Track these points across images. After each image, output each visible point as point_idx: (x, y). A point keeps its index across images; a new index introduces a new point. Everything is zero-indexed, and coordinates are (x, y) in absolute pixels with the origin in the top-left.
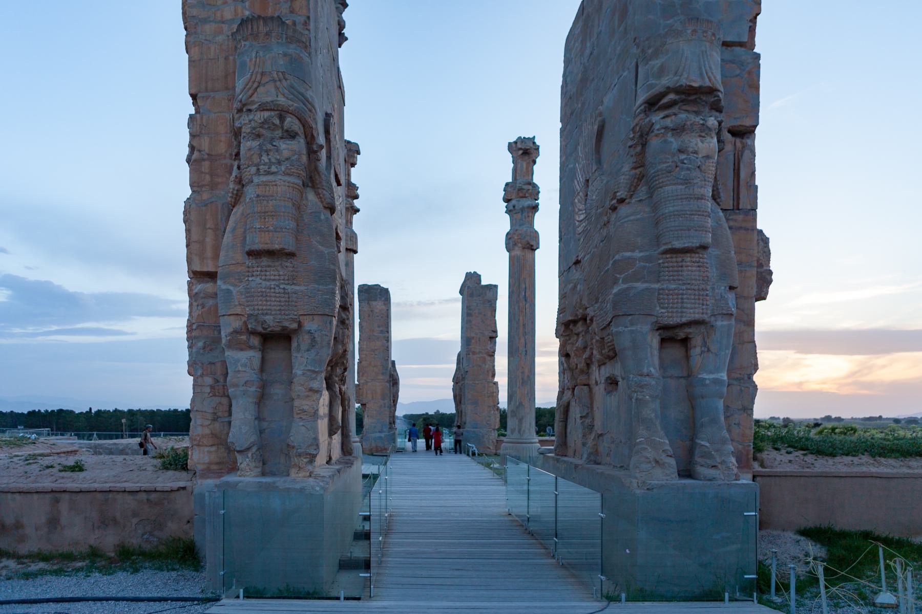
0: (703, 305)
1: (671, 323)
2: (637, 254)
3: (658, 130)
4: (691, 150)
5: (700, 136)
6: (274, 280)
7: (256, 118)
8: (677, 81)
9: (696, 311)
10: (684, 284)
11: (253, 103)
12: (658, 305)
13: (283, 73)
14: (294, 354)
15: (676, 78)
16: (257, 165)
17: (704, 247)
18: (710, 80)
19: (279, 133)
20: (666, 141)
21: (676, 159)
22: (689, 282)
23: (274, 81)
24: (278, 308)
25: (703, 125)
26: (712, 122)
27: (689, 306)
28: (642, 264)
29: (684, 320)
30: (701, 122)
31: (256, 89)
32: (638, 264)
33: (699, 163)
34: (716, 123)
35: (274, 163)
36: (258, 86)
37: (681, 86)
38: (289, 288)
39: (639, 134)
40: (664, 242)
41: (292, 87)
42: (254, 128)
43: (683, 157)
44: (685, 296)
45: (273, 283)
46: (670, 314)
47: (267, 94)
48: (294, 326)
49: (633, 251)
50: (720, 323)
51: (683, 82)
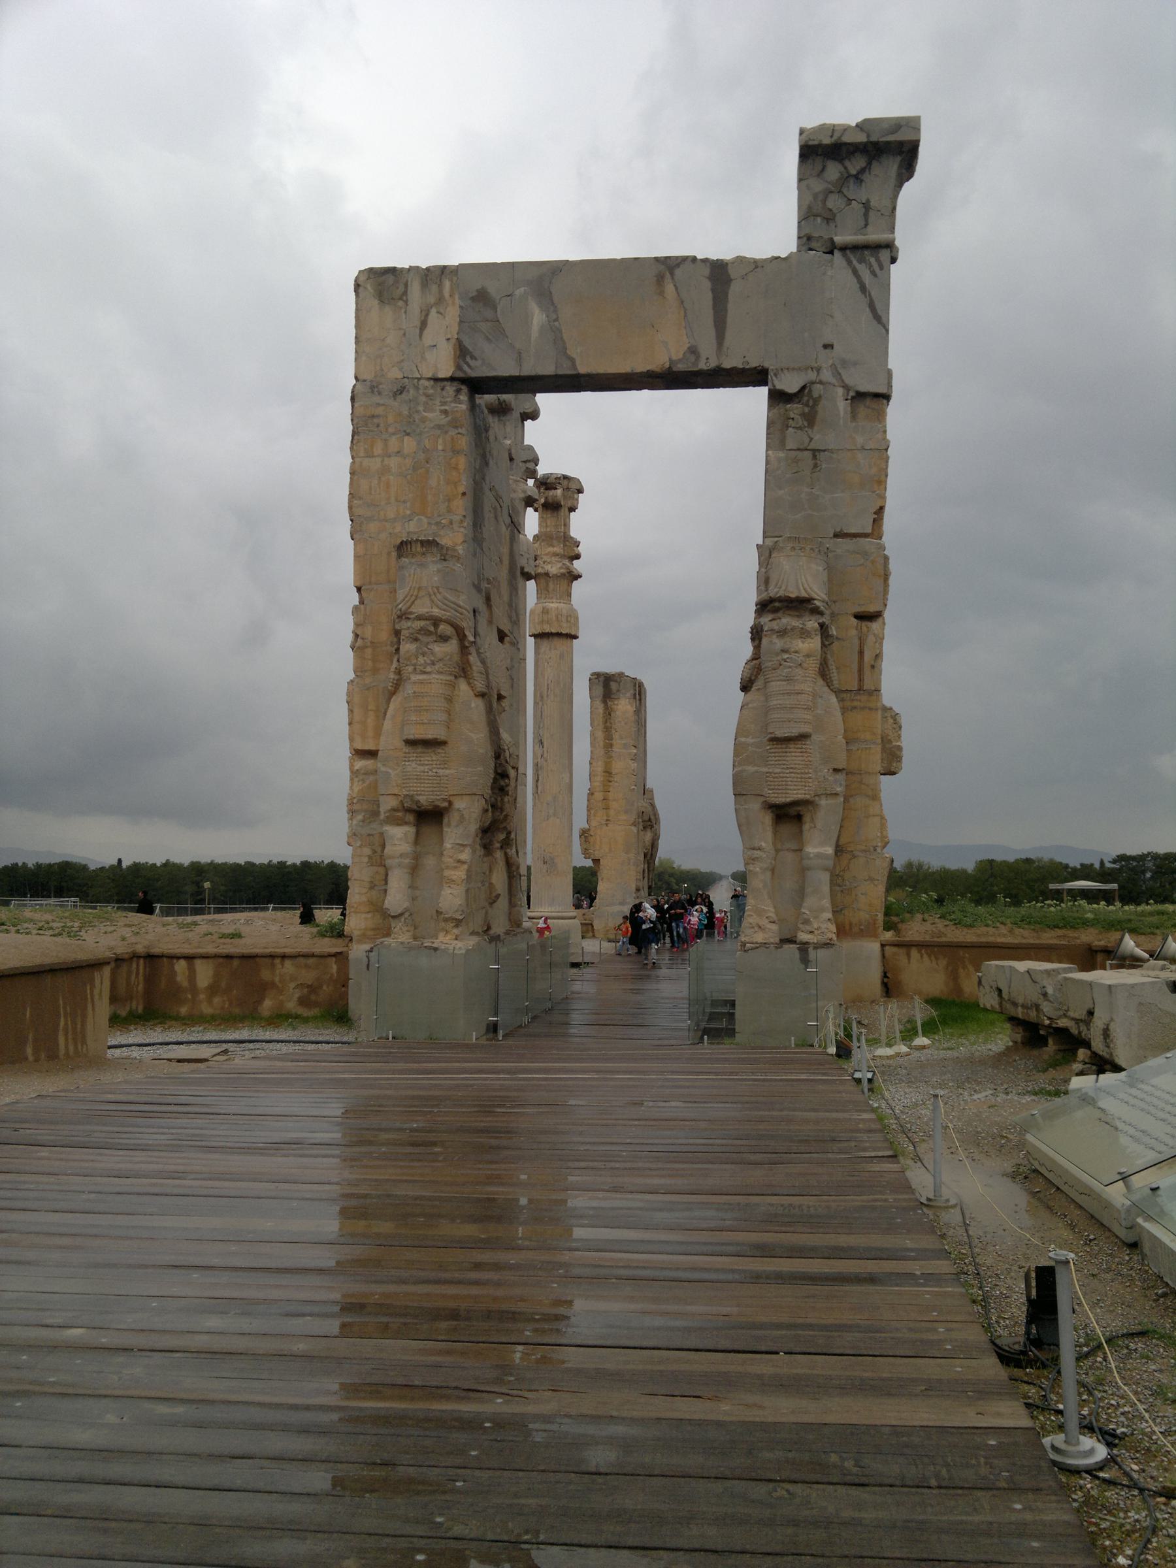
4: (793, 650)
6: (427, 765)
7: (413, 626)
8: (777, 593)
9: (799, 792)
10: (787, 768)
13: (438, 588)
14: (445, 829)
15: (776, 590)
17: (803, 737)
18: (806, 591)
21: (779, 658)
22: (792, 766)
24: (431, 789)
25: (802, 628)
26: (812, 624)
27: (792, 787)
28: (754, 749)
29: (788, 800)
30: (801, 626)
31: (413, 602)
34: (816, 625)
35: (429, 664)
36: (416, 599)
37: (780, 596)
38: (441, 772)
41: (445, 598)
42: (412, 634)
43: (786, 656)
44: (789, 779)
45: (427, 767)
46: (776, 795)
47: (422, 607)
48: (445, 804)
49: (747, 737)
50: (823, 802)
51: (781, 593)
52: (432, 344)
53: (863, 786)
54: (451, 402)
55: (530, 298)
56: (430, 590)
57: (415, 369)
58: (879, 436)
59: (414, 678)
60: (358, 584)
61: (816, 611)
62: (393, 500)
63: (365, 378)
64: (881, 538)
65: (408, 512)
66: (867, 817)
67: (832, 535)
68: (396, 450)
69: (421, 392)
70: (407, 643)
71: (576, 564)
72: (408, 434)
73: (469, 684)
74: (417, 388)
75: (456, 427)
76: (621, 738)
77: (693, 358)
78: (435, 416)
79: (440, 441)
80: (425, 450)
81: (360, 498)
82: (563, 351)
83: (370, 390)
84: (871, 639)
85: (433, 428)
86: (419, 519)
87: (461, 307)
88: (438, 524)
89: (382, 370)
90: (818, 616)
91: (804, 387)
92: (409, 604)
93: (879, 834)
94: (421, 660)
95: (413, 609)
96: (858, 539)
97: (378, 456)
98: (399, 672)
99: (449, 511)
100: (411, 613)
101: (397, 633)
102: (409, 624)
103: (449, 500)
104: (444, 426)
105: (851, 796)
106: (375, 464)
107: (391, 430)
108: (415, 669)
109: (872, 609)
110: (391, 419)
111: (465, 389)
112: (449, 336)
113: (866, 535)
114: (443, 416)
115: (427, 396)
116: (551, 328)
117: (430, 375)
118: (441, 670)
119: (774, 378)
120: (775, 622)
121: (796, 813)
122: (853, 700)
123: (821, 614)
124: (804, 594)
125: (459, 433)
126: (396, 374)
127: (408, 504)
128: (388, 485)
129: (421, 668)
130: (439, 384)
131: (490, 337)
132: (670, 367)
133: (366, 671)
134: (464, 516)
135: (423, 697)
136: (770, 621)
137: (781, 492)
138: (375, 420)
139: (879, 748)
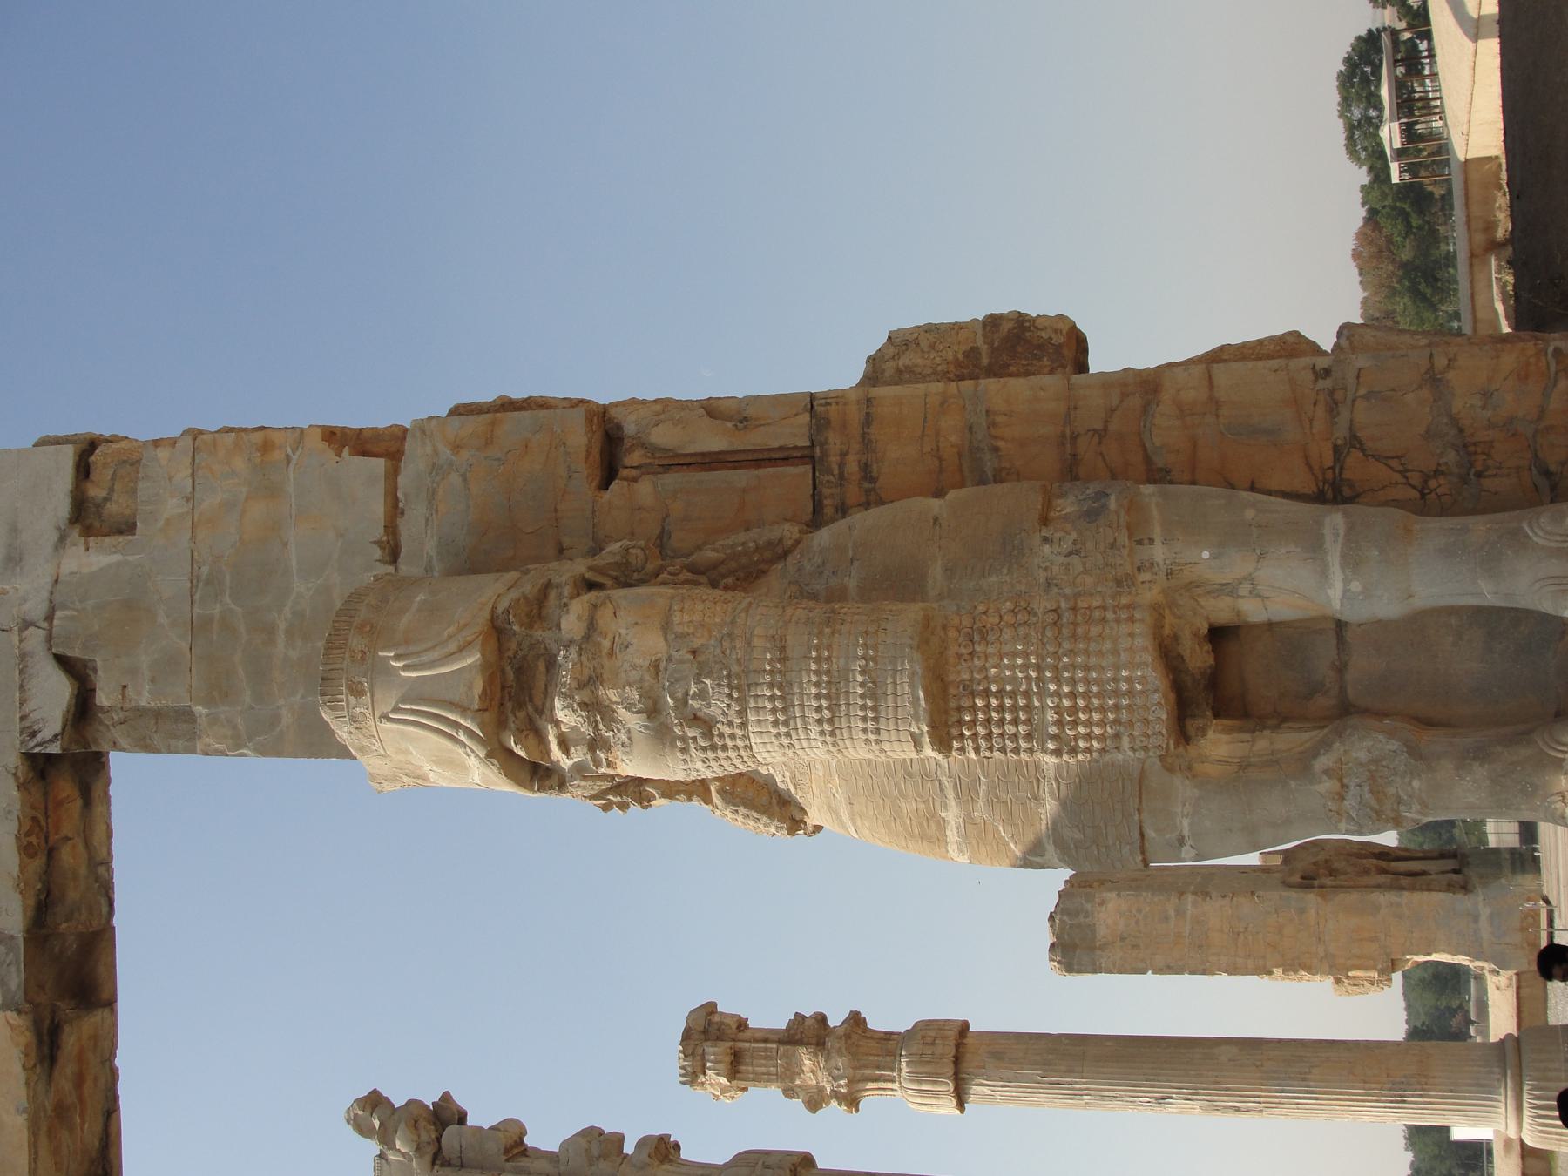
0: (1104, 620)
1: (1164, 717)
2: (952, 814)
4: (647, 677)
12: (1107, 758)
15: (462, 737)
32: (980, 811)
39: (611, 797)
40: (914, 755)
53: (1113, 427)
64: (406, 430)
66: (1215, 403)
71: (834, 1021)
76: (1167, 919)
84: (663, 436)
93: (1274, 363)
96: (400, 495)
105: (1148, 460)
109: (579, 438)
121: (1208, 647)
122: (841, 476)
137: (287, 718)
139: (990, 385)
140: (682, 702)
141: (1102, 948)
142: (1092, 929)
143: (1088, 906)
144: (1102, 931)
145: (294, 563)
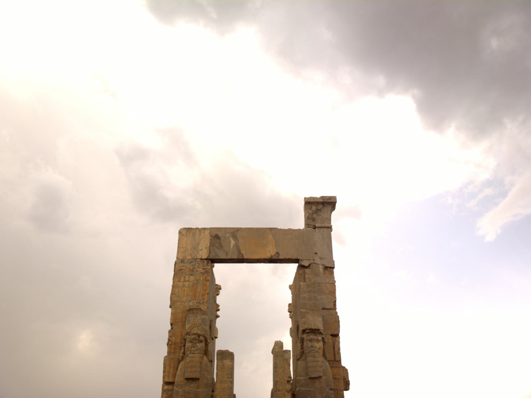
3: (306, 340)
5: (317, 342)
8: (309, 327)
11: (191, 333)
13: (200, 324)
15: (308, 326)
16: (191, 351)
19: (197, 341)
20: (307, 344)
21: (310, 349)
23: (198, 327)
26: (320, 338)
30: (317, 338)
31: (192, 329)
33: (317, 350)
34: (321, 338)
41: (202, 328)
42: (191, 340)
43: (312, 348)
47: (195, 331)
51: (310, 327)
52: (201, 249)
54: (206, 266)
55: (231, 238)
56: (198, 325)
57: (195, 256)
58: (333, 279)
59: (190, 355)
60: (172, 323)
61: (321, 333)
62: (185, 295)
63: (179, 258)
65: (190, 299)
67: (321, 309)
68: (188, 280)
69: (197, 262)
70: (188, 343)
71: (218, 313)
72: (192, 275)
73: (207, 357)
74: (196, 262)
75: (207, 273)
77: (277, 255)
78: (201, 270)
79: (202, 277)
80: (197, 280)
81: (175, 295)
82: (240, 252)
83: (181, 262)
84: (336, 343)
85: (200, 273)
86: (193, 302)
87: (210, 239)
88: (199, 303)
89: (185, 256)
90: (321, 335)
91: (310, 265)
92: (190, 330)
94: (193, 349)
95: (192, 331)
97: (182, 281)
98: (184, 353)
99: (203, 299)
100: (191, 333)
101: (185, 340)
102: (190, 336)
103: (203, 295)
104: (203, 273)
106: (181, 284)
107: (187, 274)
108: (191, 352)
109: (336, 333)
110: (187, 270)
111: (210, 262)
112: (206, 247)
113: (332, 309)
114: (203, 270)
115: (198, 263)
116: (236, 245)
117: (200, 258)
118: (199, 353)
119: (301, 262)
120: (308, 337)
122: (333, 364)
123: (322, 334)
124: (317, 328)
125: (208, 275)
126: (189, 257)
127: (190, 297)
128: (184, 291)
129: (193, 352)
130: (202, 260)
131: (219, 248)
132: (271, 258)
133: (171, 353)
134: (208, 300)
135: (193, 362)
136: (307, 336)
137: (305, 295)
138: (182, 271)
140: (312, 350)
141: (222, 361)
142: (226, 359)
143: (230, 358)
144: (225, 361)
145: (322, 296)
